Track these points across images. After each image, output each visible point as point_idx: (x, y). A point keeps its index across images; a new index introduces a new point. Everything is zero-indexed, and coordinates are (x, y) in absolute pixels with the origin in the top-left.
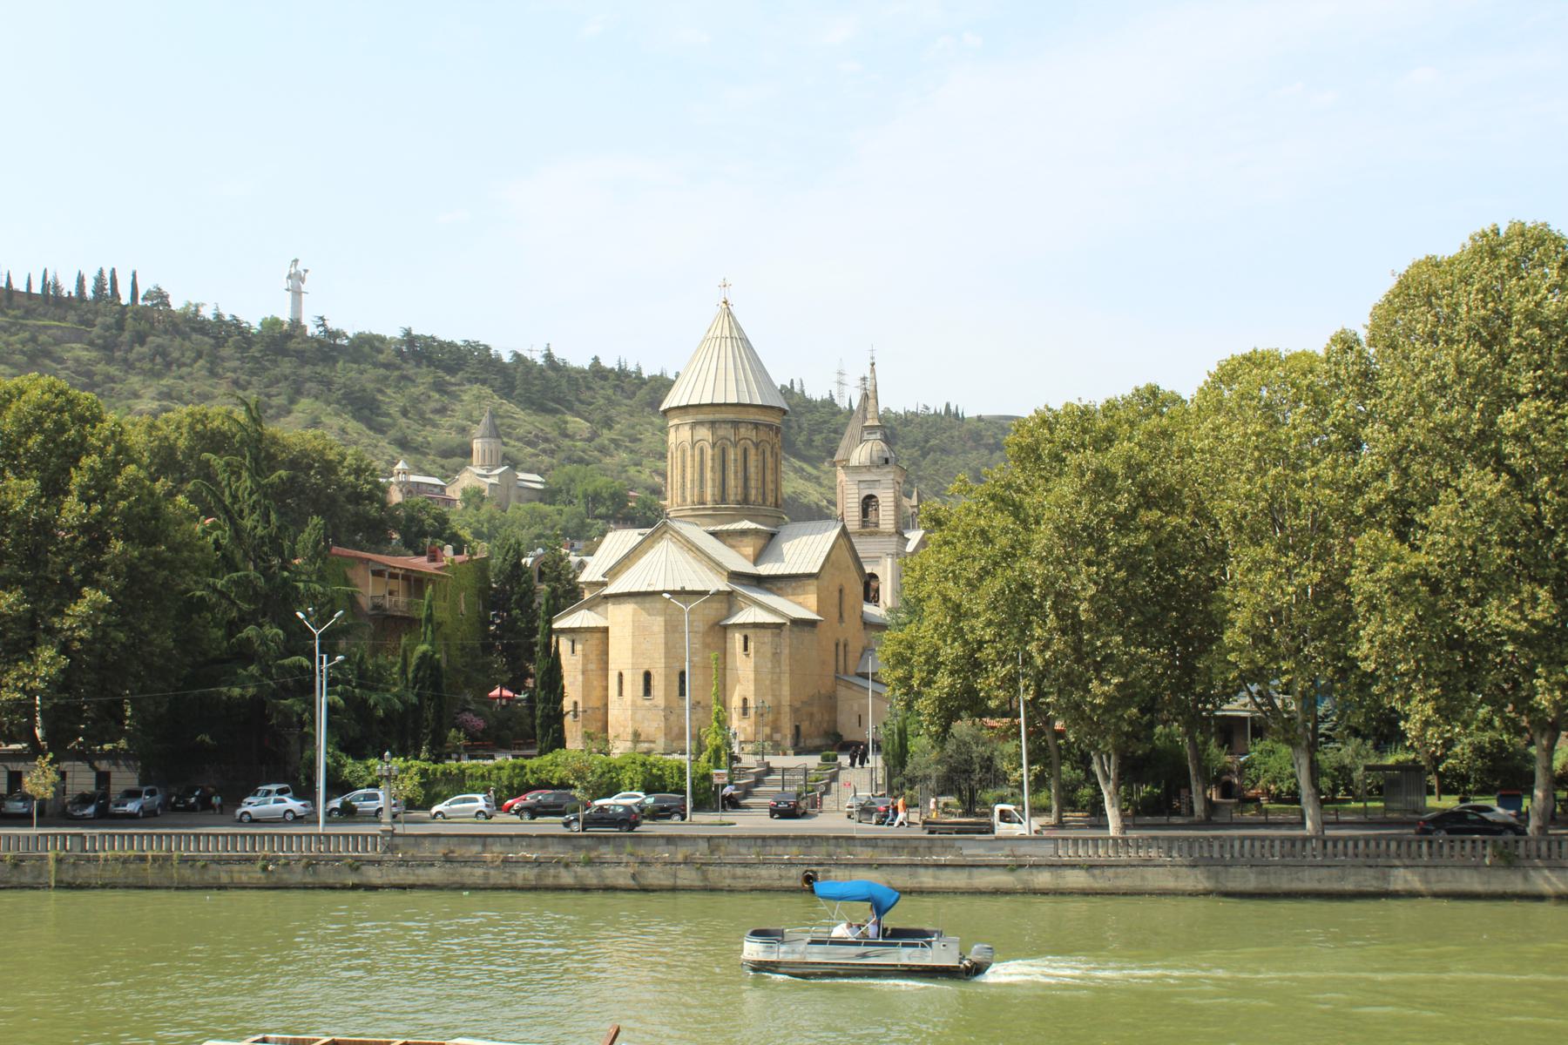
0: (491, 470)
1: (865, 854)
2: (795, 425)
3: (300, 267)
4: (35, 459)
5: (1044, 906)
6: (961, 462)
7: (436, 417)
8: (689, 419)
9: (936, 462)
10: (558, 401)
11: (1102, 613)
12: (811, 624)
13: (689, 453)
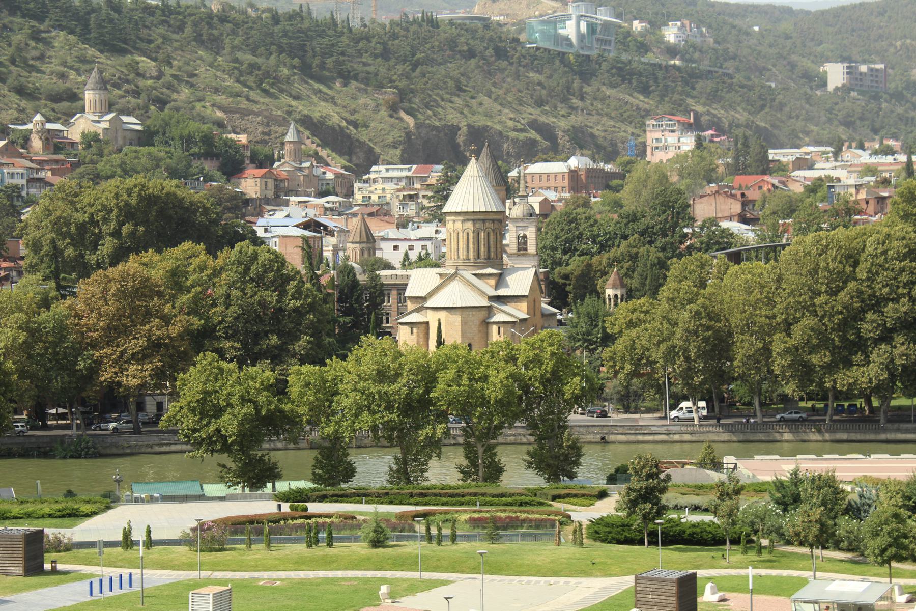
0: (102, 117)
1: (621, 430)
2: (309, 49)
4: (273, 282)
5: (678, 446)
6: (443, 72)
7: (37, 63)
8: (461, 218)
9: (424, 76)
10: (125, 41)
11: (698, 357)
12: (525, 320)
13: (461, 234)
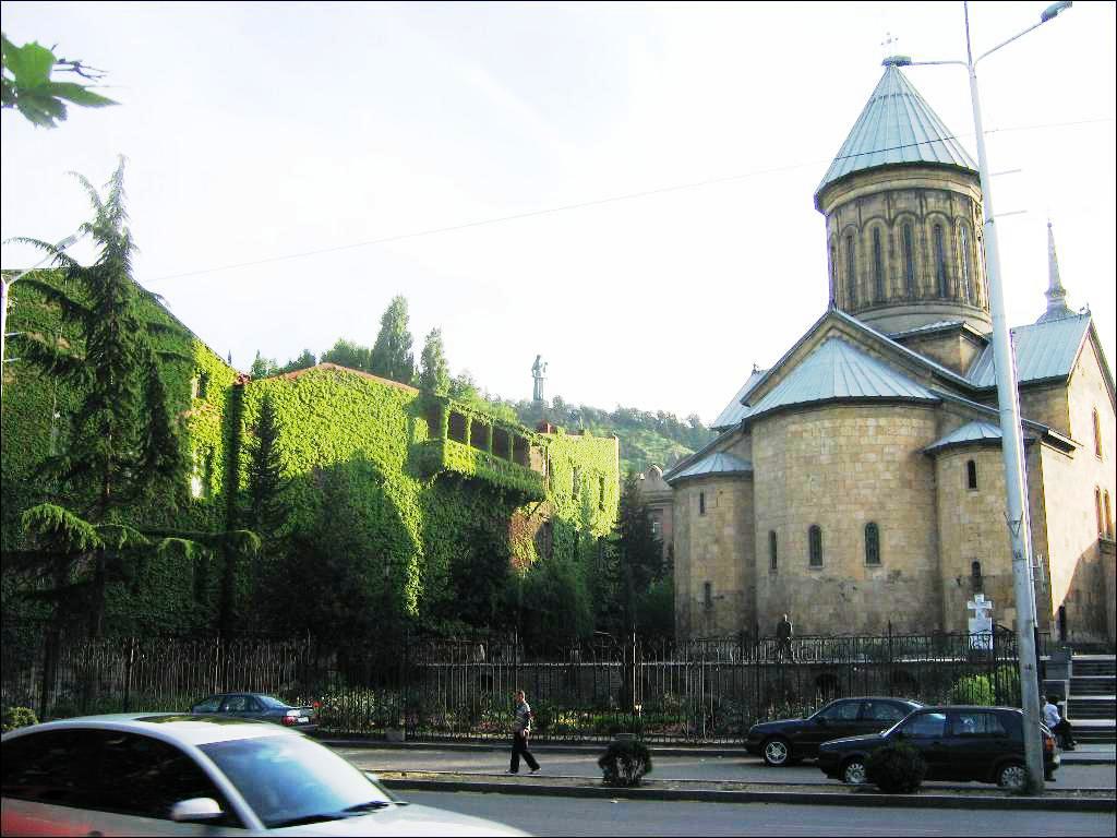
3: (541, 361)
